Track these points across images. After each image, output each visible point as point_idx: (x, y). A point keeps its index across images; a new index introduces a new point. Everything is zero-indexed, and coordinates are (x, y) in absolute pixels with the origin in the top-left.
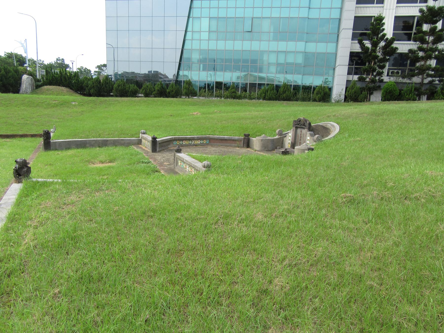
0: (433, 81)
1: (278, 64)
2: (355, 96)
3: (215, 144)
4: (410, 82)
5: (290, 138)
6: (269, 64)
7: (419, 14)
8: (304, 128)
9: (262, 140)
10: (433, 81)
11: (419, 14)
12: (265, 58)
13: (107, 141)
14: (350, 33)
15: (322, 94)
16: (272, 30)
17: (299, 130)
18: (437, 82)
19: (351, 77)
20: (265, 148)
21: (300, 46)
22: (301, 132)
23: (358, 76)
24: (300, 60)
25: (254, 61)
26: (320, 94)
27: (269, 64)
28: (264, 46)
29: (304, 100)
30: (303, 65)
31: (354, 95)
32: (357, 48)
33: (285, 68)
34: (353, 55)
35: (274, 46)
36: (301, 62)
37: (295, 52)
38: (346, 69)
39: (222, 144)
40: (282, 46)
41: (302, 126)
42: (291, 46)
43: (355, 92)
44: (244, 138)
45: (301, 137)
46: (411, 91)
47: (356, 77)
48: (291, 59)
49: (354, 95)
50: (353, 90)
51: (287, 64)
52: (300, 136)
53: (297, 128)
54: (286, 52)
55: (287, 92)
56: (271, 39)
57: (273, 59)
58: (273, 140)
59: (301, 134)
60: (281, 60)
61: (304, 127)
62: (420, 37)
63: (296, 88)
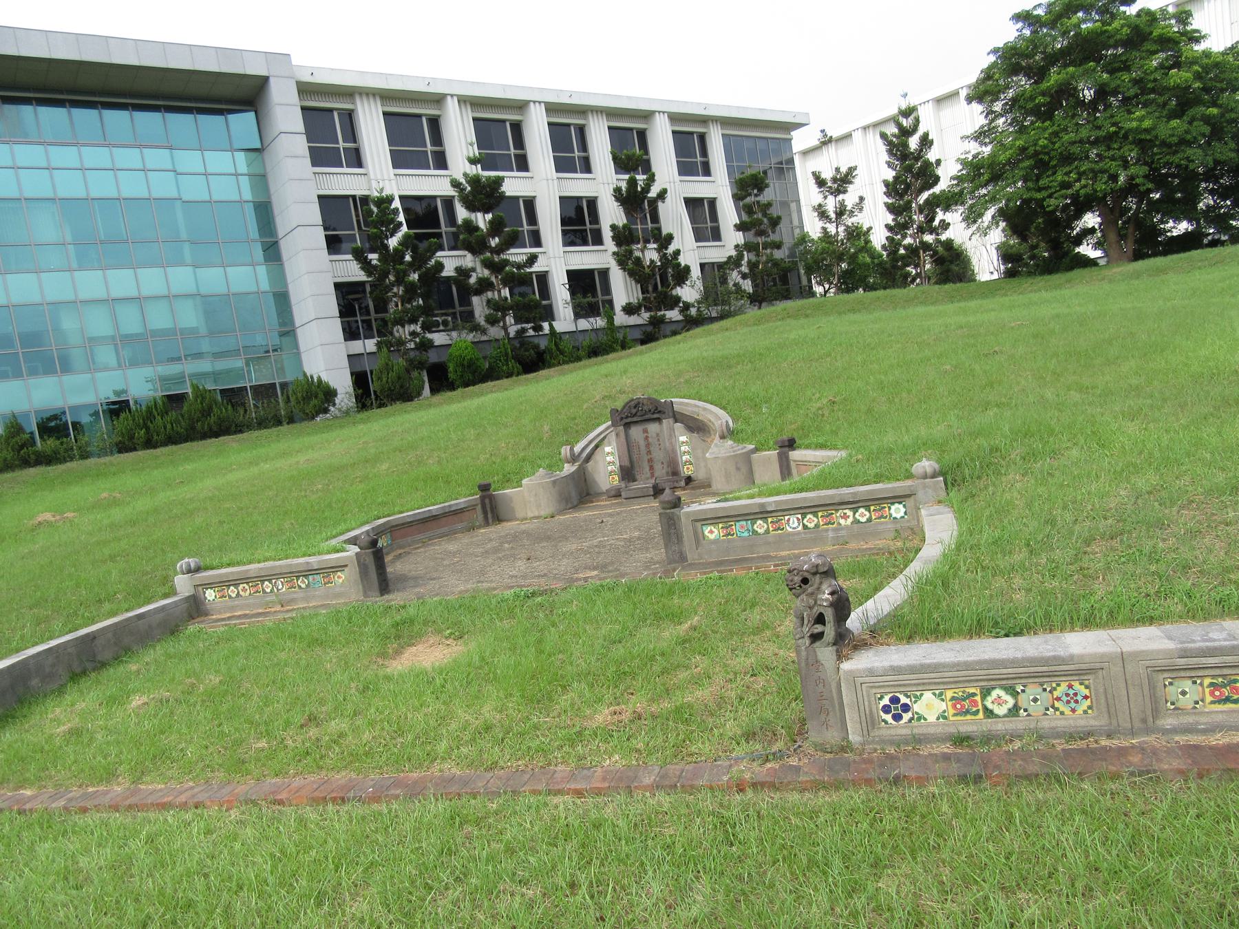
0: (524, 330)
1: (122, 341)
2: (402, 387)
3: (409, 539)
4: (484, 338)
5: (609, 459)
6: (92, 342)
7: (450, 191)
8: (659, 420)
9: (554, 482)
10: (524, 330)
11: (450, 191)
12: (69, 323)
13: (91, 637)
14: (320, 236)
15: (321, 396)
16: (69, 238)
17: (636, 432)
18: (531, 332)
19: (357, 346)
20: (567, 502)
21: (182, 278)
22: (645, 431)
23: (374, 341)
24: (190, 317)
25: (32, 339)
26: (316, 397)
27: (91, 339)
28: (56, 287)
29: (262, 424)
30: (203, 331)
31: (371, 391)
32: (353, 272)
33: (135, 348)
34: (345, 291)
35: (91, 283)
36: (195, 325)
37: (170, 298)
38: (336, 326)
39: (428, 534)
40: (122, 282)
41: (647, 417)
42: (152, 280)
43: (399, 378)
44: (483, 499)
45: (648, 445)
46: (507, 354)
47: (370, 345)
48: (159, 319)
49: (371, 391)
50: (393, 375)
51: (155, 333)
52: (642, 443)
53: (627, 426)
54: (139, 301)
55: (215, 410)
56: (75, 266)
57: (99, 324)
58: (571, 476)
59: (647, 438)
60: (130, 322)
61: (656, 416)
62: (469, 239)
63: (233, 396)
